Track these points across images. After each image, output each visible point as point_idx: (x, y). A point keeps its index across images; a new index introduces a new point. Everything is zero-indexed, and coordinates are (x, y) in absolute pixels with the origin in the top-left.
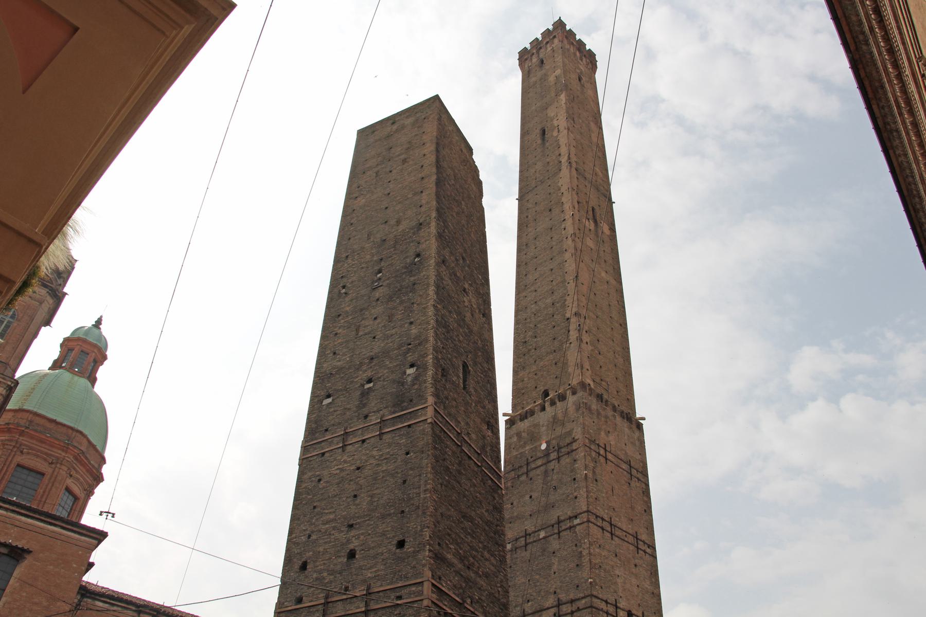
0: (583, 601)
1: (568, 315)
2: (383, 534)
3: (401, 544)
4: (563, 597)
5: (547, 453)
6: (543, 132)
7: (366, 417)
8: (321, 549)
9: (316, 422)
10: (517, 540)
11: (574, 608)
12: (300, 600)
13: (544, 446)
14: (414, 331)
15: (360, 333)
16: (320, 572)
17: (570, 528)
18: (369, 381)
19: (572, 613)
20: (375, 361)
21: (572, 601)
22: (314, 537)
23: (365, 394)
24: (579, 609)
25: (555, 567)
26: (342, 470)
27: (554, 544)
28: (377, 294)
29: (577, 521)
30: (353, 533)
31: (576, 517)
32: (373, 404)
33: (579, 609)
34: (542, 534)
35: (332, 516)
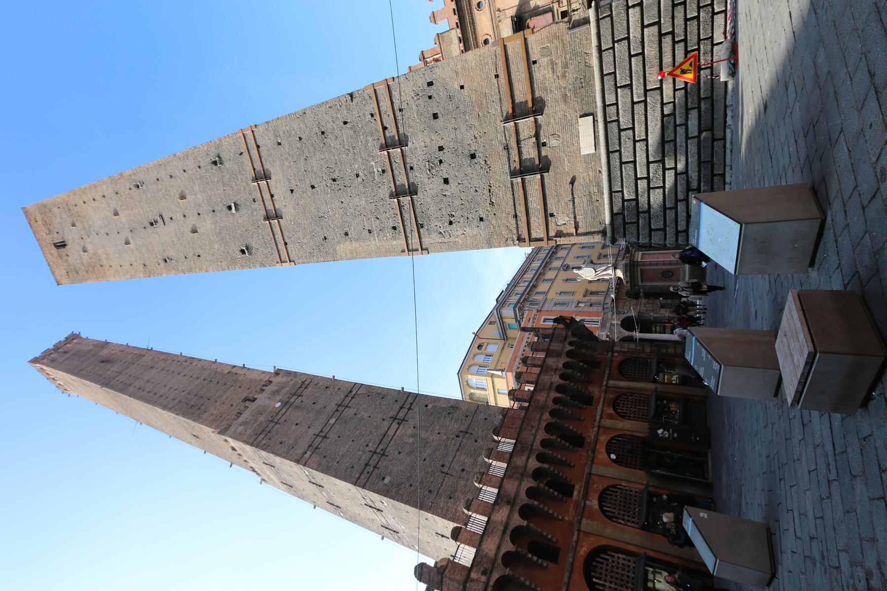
0: (410, 399)
1: (226, 372)
4: (392, 413)
5: (285, 404)
6: (102, 362)
10: (310, 446)
11: (407, 406)
13: (279, 404)
17: (352, 398)
19: (409, 409)
21: (401, 408)
24: (411, 404)
25: (366, 415)
27: (349, 412)
29: (353, 393)
31: (351, 392)
33: (411, 404)
34: (332, 421)
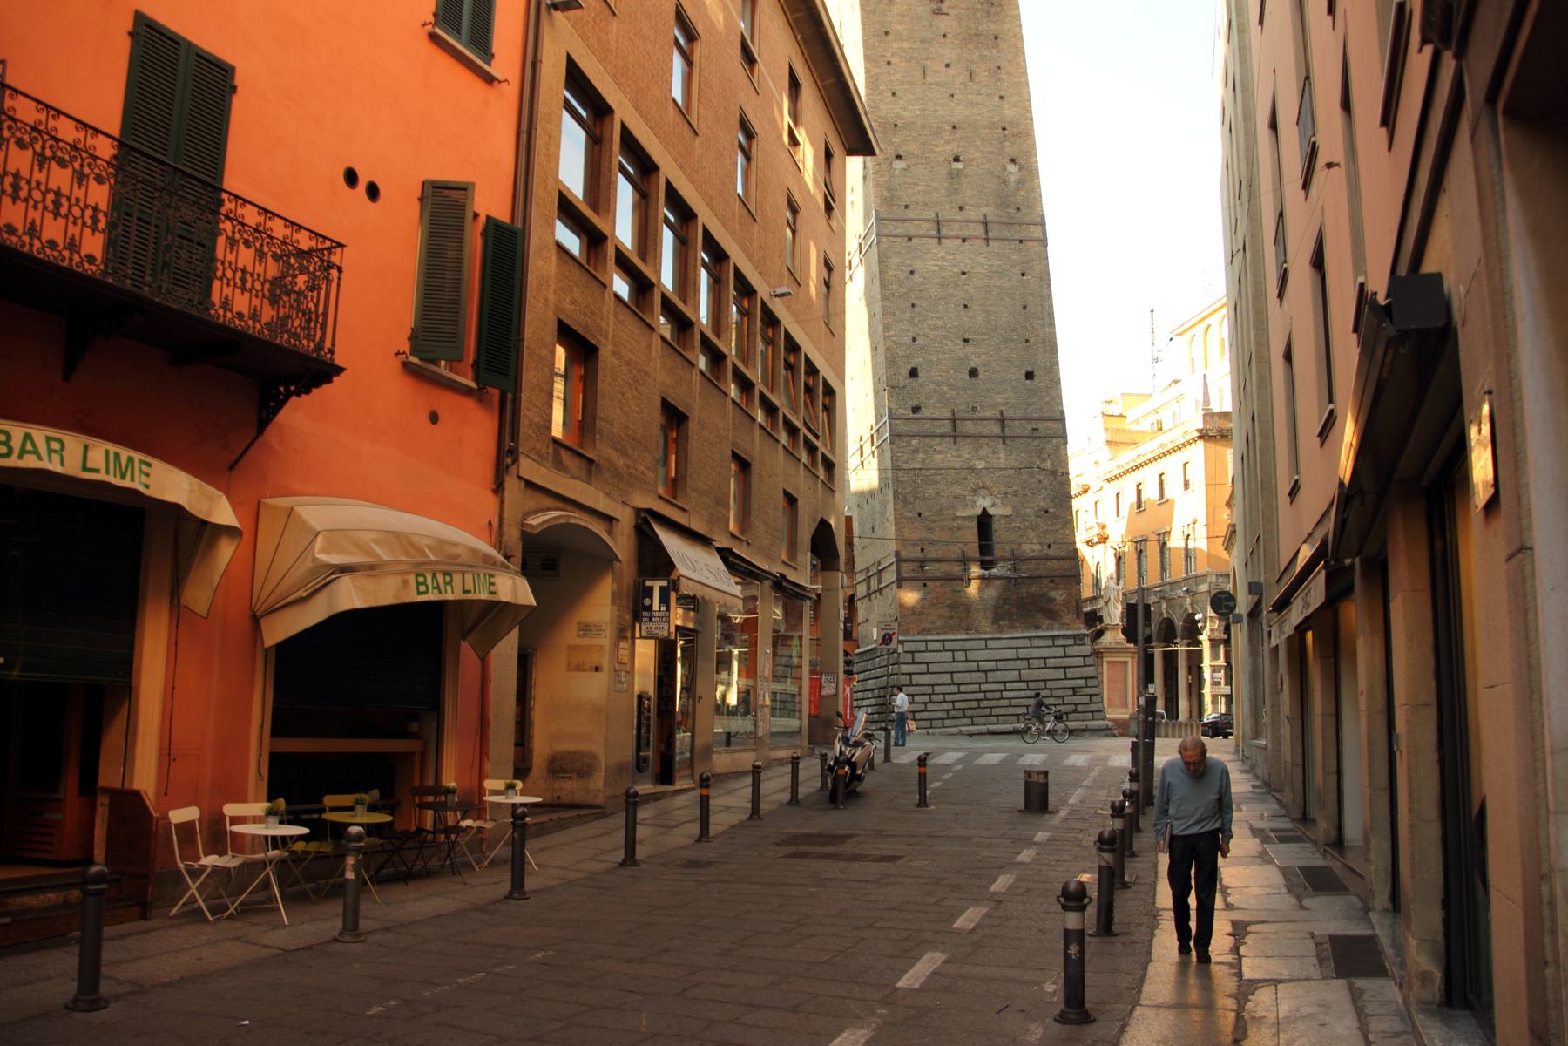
2: (1009, 360)
3: (1029, 376)
7: (961, 208)
8: (934, 358)
9: (889, 190)
12: (916, 409)
14: (1008, 112)
15: (929, 80)
16: (938, 384)
18: (957, 159)
20: (959, 134)
22: (920, 341)
23: (953, 176)
26: (941, 268)
28: (944, 24)
30: (970, 349)
32: (967, 194)
35: (940, 323)
